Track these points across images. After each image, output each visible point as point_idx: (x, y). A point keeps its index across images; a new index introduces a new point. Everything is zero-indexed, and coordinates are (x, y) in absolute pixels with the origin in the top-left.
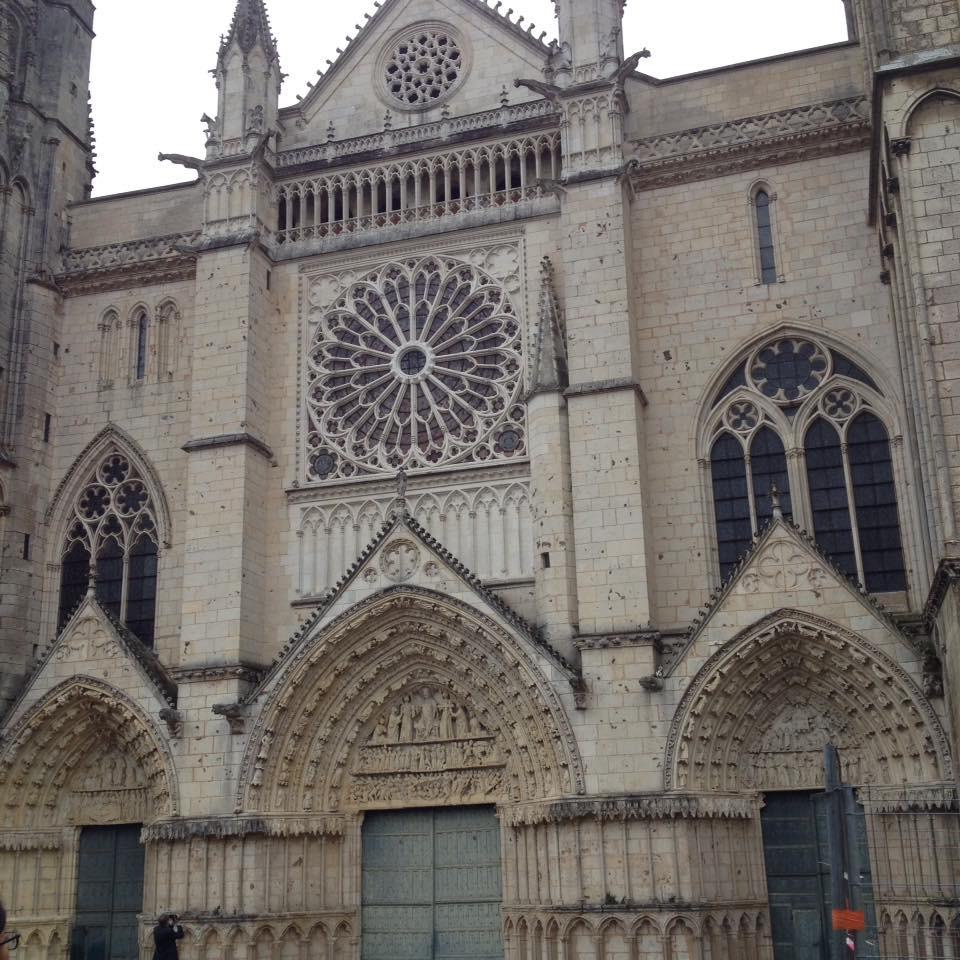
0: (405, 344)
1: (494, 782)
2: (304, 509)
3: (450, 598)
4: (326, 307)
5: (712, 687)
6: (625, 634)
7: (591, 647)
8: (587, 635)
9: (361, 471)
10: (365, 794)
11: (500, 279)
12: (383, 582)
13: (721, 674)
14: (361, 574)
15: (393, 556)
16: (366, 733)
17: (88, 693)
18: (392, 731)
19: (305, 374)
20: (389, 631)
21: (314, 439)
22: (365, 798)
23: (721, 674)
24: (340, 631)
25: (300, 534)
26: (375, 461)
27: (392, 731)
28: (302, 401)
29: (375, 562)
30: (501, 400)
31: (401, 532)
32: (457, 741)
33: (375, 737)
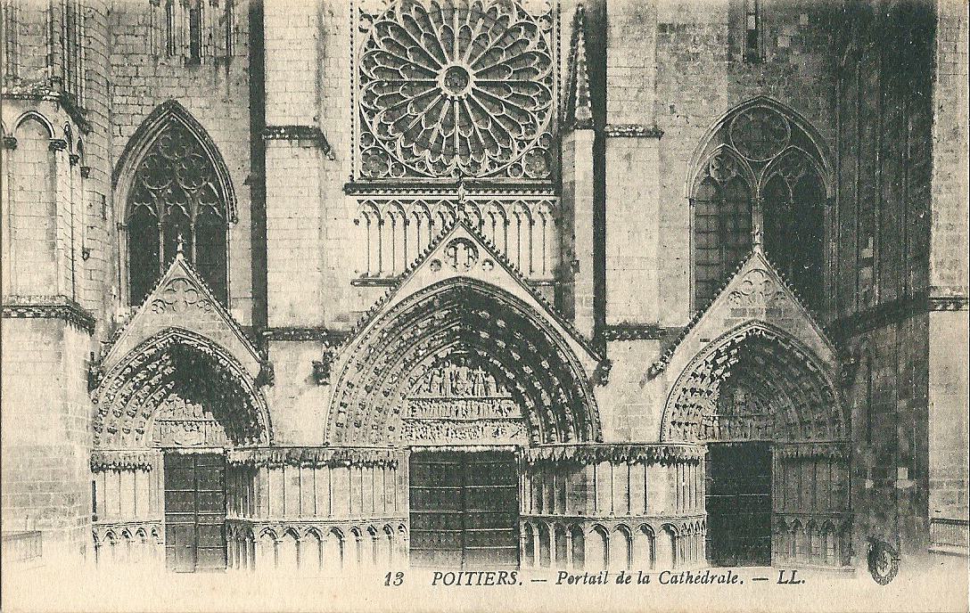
0: (450, 64)
1: (517, 430)
2: (360, 202)
3: (503, 290)
4: (376, 17)
5: (699, 371)
6: (640, 328)
7: (612, 338)
8: (613, 328)
9: (410, 172)
10: (414, 434)
11: (536, 18)
12: (447, 272)
13: (707, 363)
14: (427, 264)
15: (451, 251)
16: (415, 388)
17: (186, 342)
18: (436, 388)
19: (357, 77)
20: (447, 312)
21: (368, 137)
22: (414, 437)
23: (707, 363)
24: (409, 307)
25: (357, 222)
26: (422, 165)
27: (436, 388)
28: (355, 104)
29: (438, 254)
30: (534, 125)
31: (460, 232)
32: (489, 399)
33: (421, 391)
